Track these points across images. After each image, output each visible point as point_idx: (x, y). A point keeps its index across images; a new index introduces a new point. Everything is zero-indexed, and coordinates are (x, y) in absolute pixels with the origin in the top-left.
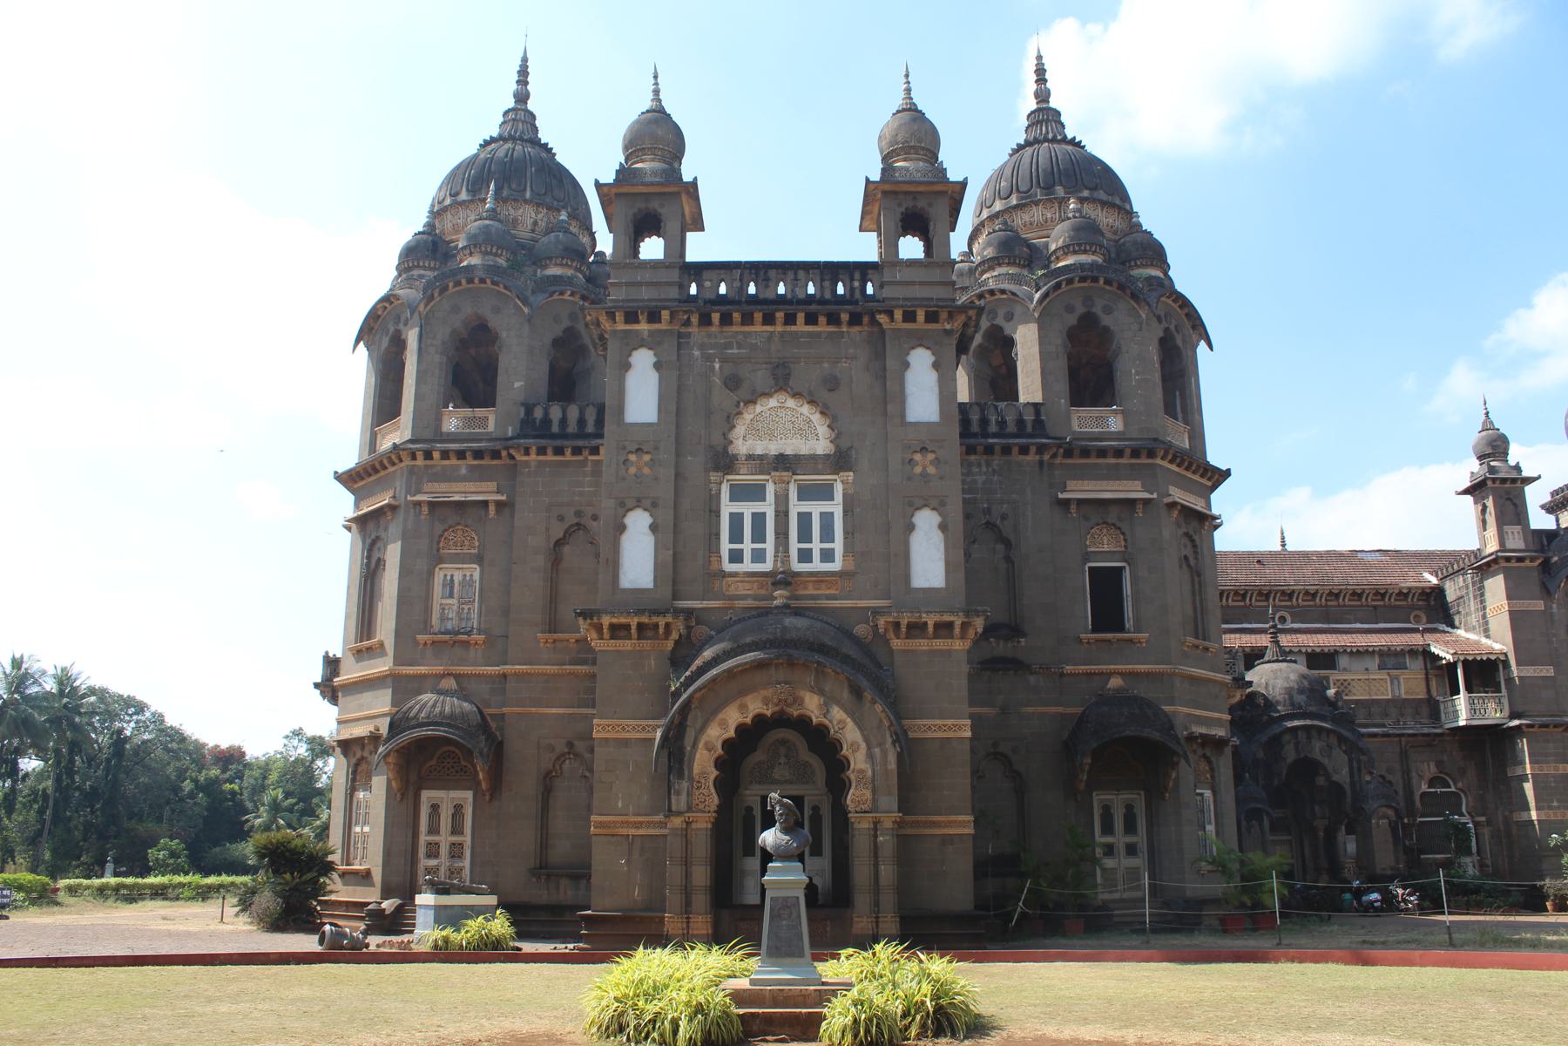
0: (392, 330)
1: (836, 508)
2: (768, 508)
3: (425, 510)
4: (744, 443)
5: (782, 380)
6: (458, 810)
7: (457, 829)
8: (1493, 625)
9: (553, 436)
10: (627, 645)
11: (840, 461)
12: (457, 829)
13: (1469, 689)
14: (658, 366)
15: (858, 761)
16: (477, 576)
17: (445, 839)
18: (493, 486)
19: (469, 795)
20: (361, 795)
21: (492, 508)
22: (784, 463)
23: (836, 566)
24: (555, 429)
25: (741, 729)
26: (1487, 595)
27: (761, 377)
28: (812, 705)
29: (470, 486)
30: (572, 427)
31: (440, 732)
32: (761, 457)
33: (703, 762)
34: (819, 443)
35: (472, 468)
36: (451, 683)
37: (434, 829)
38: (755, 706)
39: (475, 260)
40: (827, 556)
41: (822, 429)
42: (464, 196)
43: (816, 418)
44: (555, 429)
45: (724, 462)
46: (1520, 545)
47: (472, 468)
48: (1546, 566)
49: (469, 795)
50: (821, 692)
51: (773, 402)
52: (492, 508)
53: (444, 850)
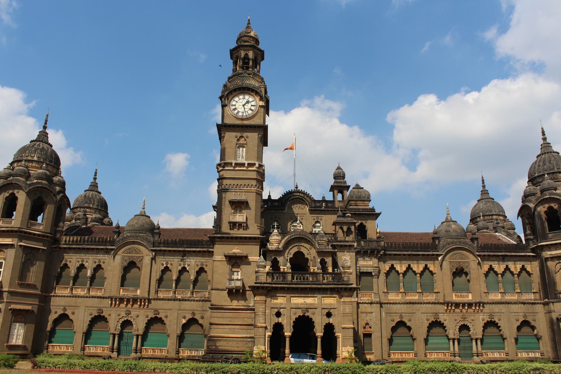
18: (42, 244)
52: (41, 251)
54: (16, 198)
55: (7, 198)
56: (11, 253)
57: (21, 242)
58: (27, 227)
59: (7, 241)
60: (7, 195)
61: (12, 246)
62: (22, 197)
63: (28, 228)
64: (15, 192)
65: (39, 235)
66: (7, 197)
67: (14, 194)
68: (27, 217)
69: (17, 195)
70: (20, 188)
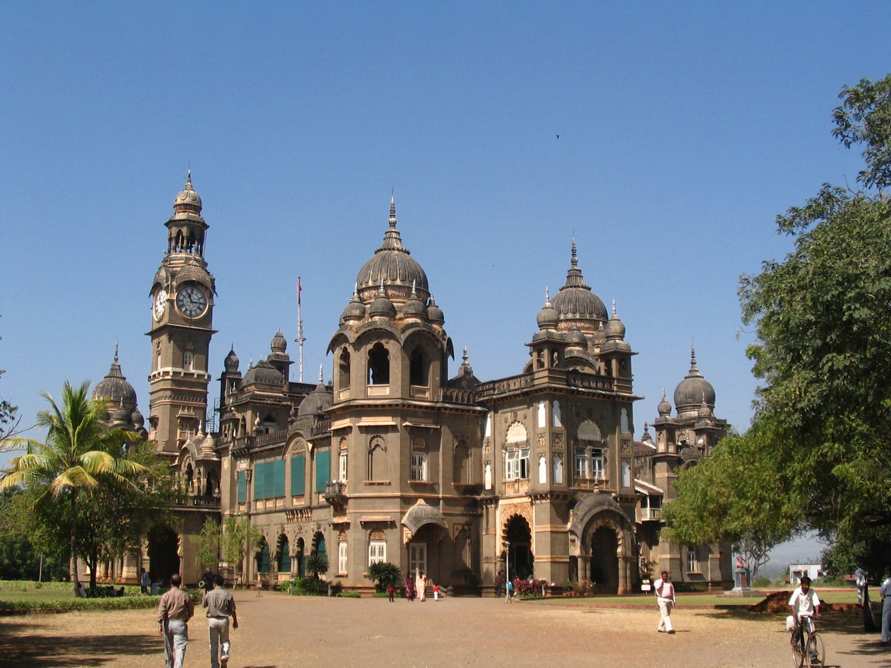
3: (409, 429)
5: (590, 416)
7: (421, 558)
8: (657, 481)
9: (452, 403)
10: (558, 501)
12: (421, 558)
13: (651, 506)
14: (560, 407)
18: (431, 421)
19: (424, 545)
20: (372, 544)
21: (432, 431)
24: (454, 401)
25: (597, 530)
26: (656, 467)
29: (422, 420)
30: (460, 401)
31: (435, 522)
32: (585, 441)
35: (423, 413)
36: (421, 501)
38: (599, 523)
41: (599, 433)
42: (398, 282)
43: (597, 429)
44: (454, 401)
46: (672, 449)
47: (423, 413)
49: (424, 545)
50: (614, 519)
51: (586, 422)
52: (432, 431)
53: (418, 565)
54: (387, 352)
55: (371, 352)
56: (393, 439)
57: (405, 420)
58: (410, 396)
59: (387, 421)
60: (370, 346)
61: (393, 428)
62: (393, 349)
63: (412, 398)
64: (383, 342)
65: (427, 407)
66: (370, 350)
67: (382, 345)
68: (408, 380)
69: (386, 346)
70: (391, 336)
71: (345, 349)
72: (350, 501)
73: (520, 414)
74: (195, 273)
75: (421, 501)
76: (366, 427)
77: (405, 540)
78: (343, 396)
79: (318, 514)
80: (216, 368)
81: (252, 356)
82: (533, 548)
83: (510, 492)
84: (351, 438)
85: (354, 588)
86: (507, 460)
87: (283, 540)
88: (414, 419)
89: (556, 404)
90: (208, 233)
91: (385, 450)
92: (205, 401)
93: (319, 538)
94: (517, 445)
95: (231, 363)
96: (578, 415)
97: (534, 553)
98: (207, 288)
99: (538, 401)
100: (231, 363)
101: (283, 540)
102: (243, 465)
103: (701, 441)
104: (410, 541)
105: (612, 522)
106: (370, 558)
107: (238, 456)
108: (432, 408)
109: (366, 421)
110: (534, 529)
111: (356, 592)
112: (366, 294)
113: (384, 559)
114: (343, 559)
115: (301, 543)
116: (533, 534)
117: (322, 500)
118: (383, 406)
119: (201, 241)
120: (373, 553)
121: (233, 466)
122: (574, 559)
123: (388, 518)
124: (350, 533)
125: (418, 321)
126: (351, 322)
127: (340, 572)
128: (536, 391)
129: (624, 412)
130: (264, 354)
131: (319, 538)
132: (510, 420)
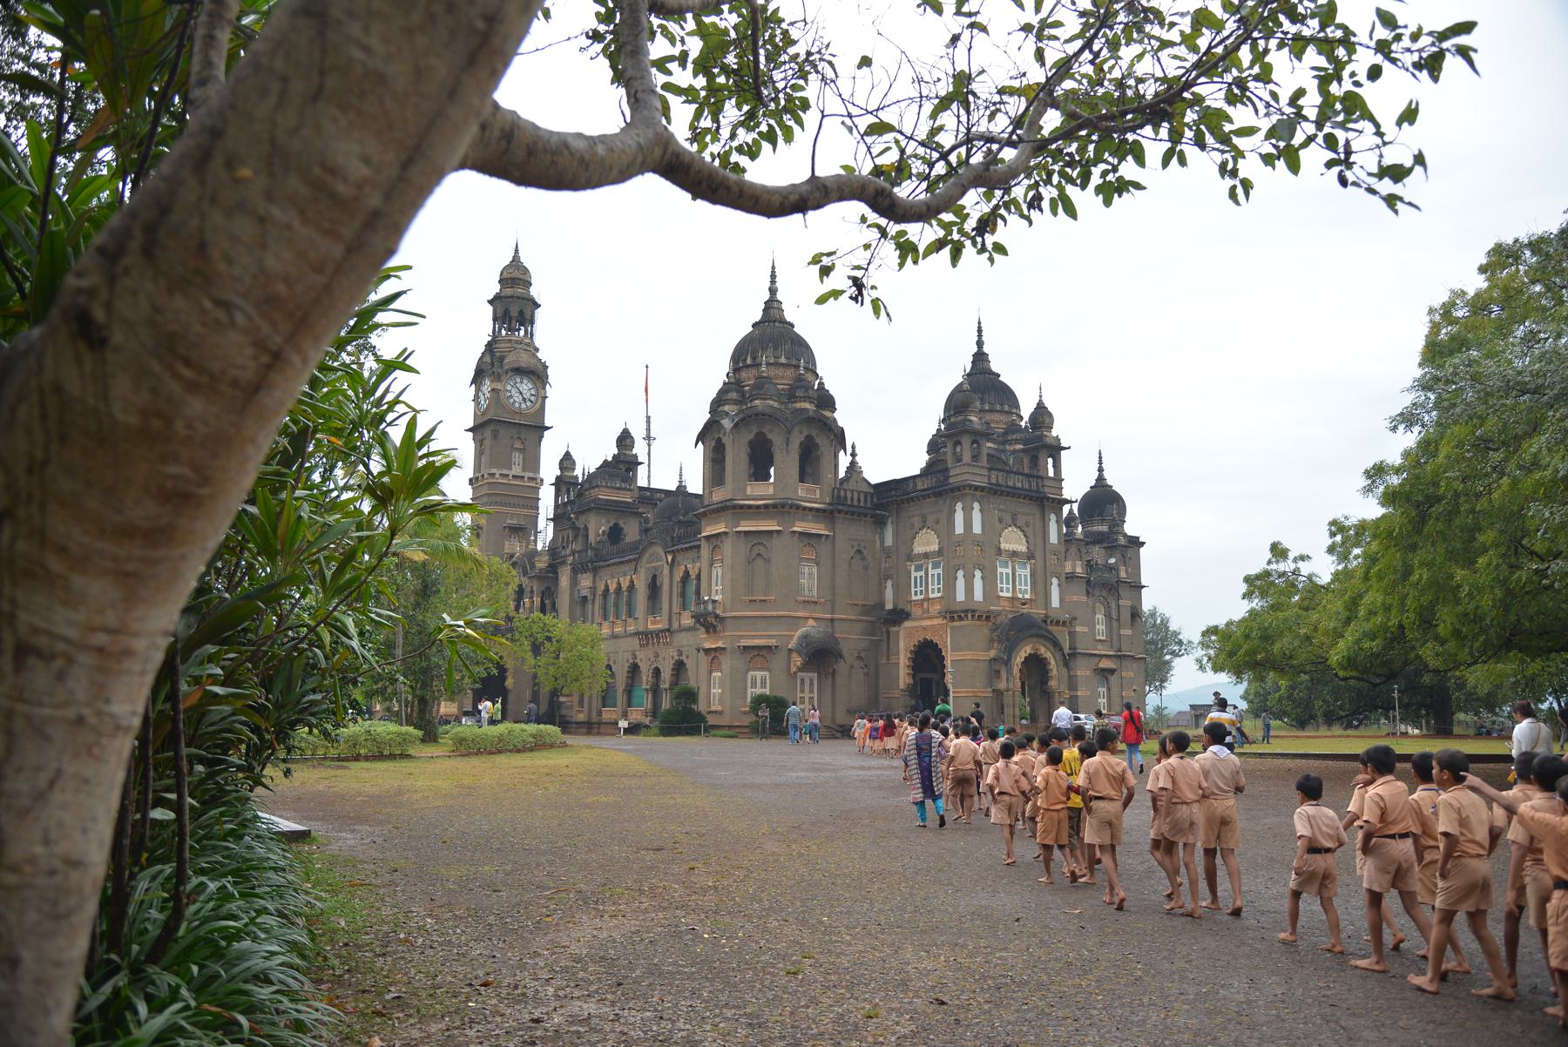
0: (755, 430)
1: (1027, 572)
2: (1009, 571)
4: (1003, 546)
6: (811, 684)
7: (811, 691)
11: (1030, 556)
12: (811, 691)
15: (1055, 672)
16: (815, 570)
17: (807, 695)
22: (1014, 554)
23: (1027, 596)
27: (1008, 519)
28: (1043, 650)
33: (1016, 670)
34: (1022, 548)
36: (811, 622)
37: (802, 691)
39: (807, 405)
40: (1025, 591)
42: (783, 360)
45: (999, 552)
48: (1088, 582)
55: (751, 442)
65: (818, 510)
69: (770, 436)
71: (719, 441)
72: (728, 622)
73: (930, 519)
74: (524, 360)
75: (811, 622)
76: (746, 533)
77: (794, 669)
78: (718, 496)
79: (683, 639)
80: (549, 470)
81: (592, 456)
82: (949, 679)
83: (917, 612)
84: (727, 547)
85: (730, 727)
86: (913, 574)
87: (634, 669)
88: (803, 524)
89: (976, 506)
90: (538, 312)
91: (767, 561)
92: (537, 508)
93: (680, 666)
94: (926, 556)
95: (567, 461)
96: (1000, 520)
97: (950, 686)
98: (539, 377)
99: (955, 500)
100: (567, 461)
101: (634, 669)
102: (585, 581)
103: (1112, 561)
104: (800, 670)
105: (1043, 650)
106: (749, 690)
107: (577, 570)
108: (824, 511)
109: (745, 526)
110: (949, 658)
111: (733, 731)
112: (744, 374)
113: (767, 691)
114: (716, 691)
115: (657, 672)
116: (948, 663)
117: (687, 621)
118: (766, 506)
119: (532, 322)
120: (754, 685)
121: (574, 582)
122: (998, 694)
123: (772, 642)
124: (726, 661)
125: (807, 405)
126: (726, 408)
127: (713, 708)
128: (952, 490)
129: (1053, 517)
130: (611, 451)
131: (680, 666)
132: (917, 526)
